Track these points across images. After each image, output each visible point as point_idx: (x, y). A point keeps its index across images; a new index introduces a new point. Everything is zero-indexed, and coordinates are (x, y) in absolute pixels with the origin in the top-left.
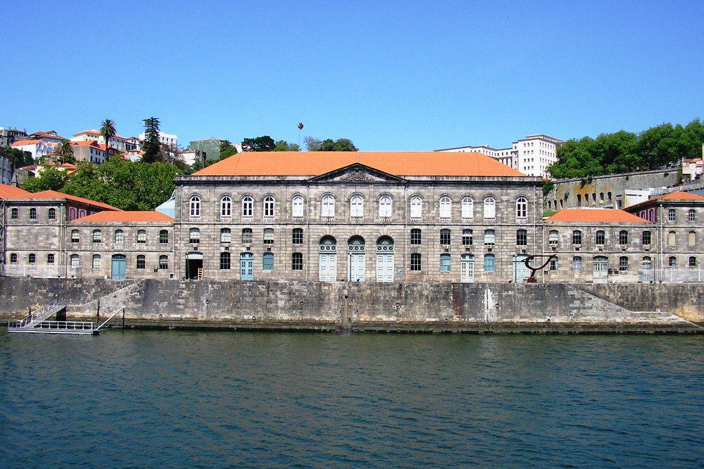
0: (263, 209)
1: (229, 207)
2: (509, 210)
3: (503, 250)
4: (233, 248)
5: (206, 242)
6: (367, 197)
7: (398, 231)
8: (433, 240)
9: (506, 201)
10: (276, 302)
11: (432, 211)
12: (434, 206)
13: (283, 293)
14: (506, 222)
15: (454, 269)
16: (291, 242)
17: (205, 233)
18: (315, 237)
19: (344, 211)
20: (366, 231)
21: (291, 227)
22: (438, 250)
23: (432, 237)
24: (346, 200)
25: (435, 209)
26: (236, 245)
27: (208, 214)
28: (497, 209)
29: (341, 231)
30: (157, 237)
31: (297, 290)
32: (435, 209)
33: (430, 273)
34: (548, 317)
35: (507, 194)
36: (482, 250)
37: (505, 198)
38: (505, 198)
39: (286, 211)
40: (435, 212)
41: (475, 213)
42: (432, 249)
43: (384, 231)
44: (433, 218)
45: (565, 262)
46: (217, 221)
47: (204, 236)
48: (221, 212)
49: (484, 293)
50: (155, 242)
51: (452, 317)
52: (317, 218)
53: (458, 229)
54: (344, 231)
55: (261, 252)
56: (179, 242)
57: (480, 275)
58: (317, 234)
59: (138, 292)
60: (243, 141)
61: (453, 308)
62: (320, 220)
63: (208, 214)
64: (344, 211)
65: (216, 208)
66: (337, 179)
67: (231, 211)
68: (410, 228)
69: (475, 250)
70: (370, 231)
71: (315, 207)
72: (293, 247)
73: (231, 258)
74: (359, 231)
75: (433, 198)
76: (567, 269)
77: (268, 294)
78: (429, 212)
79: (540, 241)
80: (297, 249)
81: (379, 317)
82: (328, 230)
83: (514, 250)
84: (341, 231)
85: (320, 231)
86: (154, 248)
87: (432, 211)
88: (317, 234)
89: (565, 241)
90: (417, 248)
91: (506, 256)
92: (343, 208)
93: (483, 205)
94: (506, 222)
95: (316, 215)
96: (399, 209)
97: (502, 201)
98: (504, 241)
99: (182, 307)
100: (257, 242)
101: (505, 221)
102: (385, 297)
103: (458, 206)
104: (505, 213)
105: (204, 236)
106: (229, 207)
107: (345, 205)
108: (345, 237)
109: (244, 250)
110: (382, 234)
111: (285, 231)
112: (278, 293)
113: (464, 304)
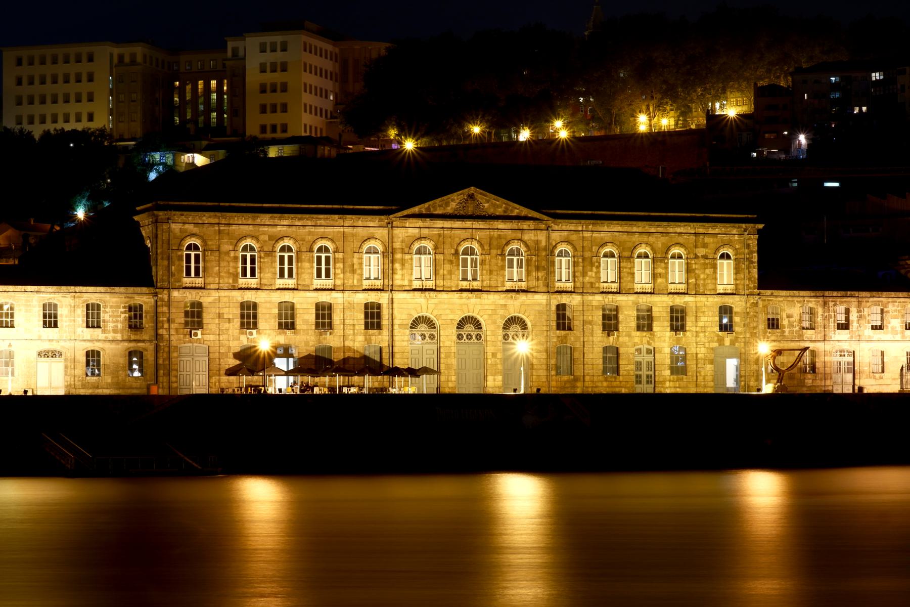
0: (312, 267)
1: (253, 261)
3: (698, 339)
7: (537, 308)
8: (591, 322)
11: (590, 273)
12: (592, 264)
17: (213, 310)
18: (404, 316)
20: (486, 307)
21: (363, 298)
24: (453, 251)
25: (594, 269)
28: (689, 270)
29: (446, 306)
30: (123, 316)
32: (594, 269)
33: (587, 378)
35: (705, 246)
36: (667, 339)
37: (701, 252)
39: (353, 271)
40: (594, 274)
41: (655, 276)
48: (240, 270)
56: (166, 326)
63: (219, 275)
65: (231, 264)
67: (257, 271)
69: (656, 339)
70: (493, 307)
71: (403, 265)
72: (365, 335)
75: (591, 251)
78: (584, 274)
79: (755, 324)
83: (716, 339)
84: (446, 306)
87: (590, 273)
89: (791, 325)
92: (447, 267)
95: (403, 279)
96: (538, 269)
97: (696, 257)
104: (702, 276)
106: (253, 261)
107: (451, 262)
111: (352, 306)
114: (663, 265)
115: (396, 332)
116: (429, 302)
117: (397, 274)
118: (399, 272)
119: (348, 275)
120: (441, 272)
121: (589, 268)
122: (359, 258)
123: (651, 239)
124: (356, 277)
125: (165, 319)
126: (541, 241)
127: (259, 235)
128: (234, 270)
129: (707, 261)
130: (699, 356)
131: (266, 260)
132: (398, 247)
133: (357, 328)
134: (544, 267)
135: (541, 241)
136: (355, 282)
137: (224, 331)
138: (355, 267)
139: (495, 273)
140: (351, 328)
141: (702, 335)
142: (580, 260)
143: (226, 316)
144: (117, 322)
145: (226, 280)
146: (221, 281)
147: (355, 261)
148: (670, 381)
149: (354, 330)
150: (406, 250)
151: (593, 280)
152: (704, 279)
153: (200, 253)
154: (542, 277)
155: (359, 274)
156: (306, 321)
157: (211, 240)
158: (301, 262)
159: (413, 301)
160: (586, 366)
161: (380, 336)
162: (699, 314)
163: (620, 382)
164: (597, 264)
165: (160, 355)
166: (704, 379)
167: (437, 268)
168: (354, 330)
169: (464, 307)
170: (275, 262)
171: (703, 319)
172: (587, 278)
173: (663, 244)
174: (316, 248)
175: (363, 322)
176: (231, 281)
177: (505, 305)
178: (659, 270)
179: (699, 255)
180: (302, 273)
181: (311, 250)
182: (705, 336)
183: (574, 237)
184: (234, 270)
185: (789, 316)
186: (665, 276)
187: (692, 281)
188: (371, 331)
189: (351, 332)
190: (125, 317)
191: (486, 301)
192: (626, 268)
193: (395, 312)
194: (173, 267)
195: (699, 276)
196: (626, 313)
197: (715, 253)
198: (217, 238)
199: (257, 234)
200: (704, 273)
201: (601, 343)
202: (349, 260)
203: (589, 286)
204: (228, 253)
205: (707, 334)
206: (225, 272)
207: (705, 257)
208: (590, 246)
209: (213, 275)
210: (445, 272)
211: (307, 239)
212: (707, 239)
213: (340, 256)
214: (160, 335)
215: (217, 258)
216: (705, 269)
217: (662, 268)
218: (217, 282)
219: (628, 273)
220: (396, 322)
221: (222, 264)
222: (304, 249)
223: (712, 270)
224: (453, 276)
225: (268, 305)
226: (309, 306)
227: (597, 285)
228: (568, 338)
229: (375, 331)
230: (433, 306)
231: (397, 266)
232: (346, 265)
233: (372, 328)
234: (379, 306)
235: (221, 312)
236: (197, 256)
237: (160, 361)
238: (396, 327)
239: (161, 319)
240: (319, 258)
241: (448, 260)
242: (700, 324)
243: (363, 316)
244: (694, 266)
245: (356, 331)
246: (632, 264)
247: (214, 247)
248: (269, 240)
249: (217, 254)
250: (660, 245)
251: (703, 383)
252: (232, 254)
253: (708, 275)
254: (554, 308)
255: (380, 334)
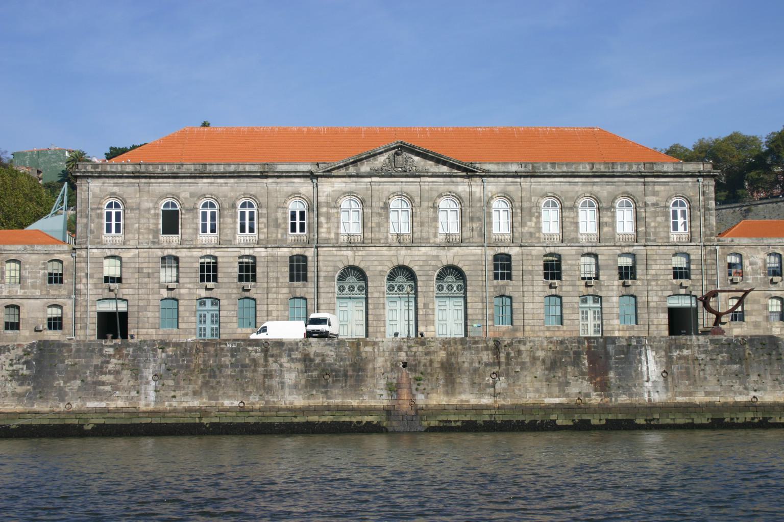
0: (235, 222)
2: (659, 219)
3: (650, 288)
4: (183, 291)
5: (133, 281)
6: (417, 200)
7: (472, 258)
8: (531, 273)
9: (653, 205)
10: (281, 376)
11: (529, 224)
13: (292, 360)
14: (655, 241)
15: (569, 322)
16: (288, 279)
17: (133, 265)
18: (330, 269)
19: (379, 225)
21: (285, 252)
22: (540, 289)
23: (530, 268)
24: (381, 204)
25: (534, 219)
26: (188, 286)
27: (138, 231)
29: (374, 258)
31: (317, 354)
32: (534, 219)
33: (527, 328)
34: (754, 394)
35: (655, 194)
36: (615, 288)
38: (651, 200)
40: (533, 225)
41: (600, 225)
42: (531, 288)
43: (449, 257)
44: (531, 234)
45: (756, 307)
46: (154, 243)
47: (130, 271)
49: (640, 354)
50: (39, 281)
51: (588, 395)
52: (332, 236)
53: (574, 252)
54: (379, 258)
55: (234, 296)
56: (84, 281)
57: (613, 331)
58: (331, 264)
59: (24, 363)
60: (108, 151)
61: (590, 380)
62: (337, 239)
63: (138, 231)
64: (379, 225)
65: (152, 221)
66: (365, 168)
68: (491, 252)
69: (603, 288)
70: (424, 258)
72: (289, 287)
73: (181, 308)
74: (405, 257)
76: (760, 319)
77: (266, 360)
78: (523, 224)
79: (713, 272)
80: (298, 290)
81: (464, 397)
82: (350, 257)
83: (669, 287)
84: (374, 258)
85: (337, 259)
86: (38, 293)
87: (529, 224)
88: (331, 264)
89: (755, 272)
90: (504, 286)
91: (655, 299)
92: (376, 219)
93: (614, 212)
94: (655, 241)
95: (329, 233)
98: (653, 272)
99: (108, 388)
100: (226, 280)
101: (652, 238)
102: (471, 363)
103: (572, 215)
104: (653, 224)
105: (130, 271)
107: (380, 215)
108: (380, 268)
109: (203, 293)
110: (445, 263)
111: (275, 260)
112: (284, 360)
113: (606, 373)
114: (609, 214)
115: (321, 284)
116: (357, 254)
117: (322, 227)
118: (325, 226)
119: (272, 229)
120: (369, 225)
121: (528, 218)
122: (283, 213)
123: (596, 189)
124: (280, 231)
125: (83, 274)
126: (475, 192)
127: (179, 193)
128: (154, 226)
129: (658, 210)
130: (651, 304)
131: (187, 216)
132: (323, 201)
133: (281, 280)
134: (478, 218)
135: (475, 192)
136: (279, 236)
137: (143, 285)
138: (280, 221)
139: (426, 225)
140: (275, 280)
141: (653, 283)
142: (519, 211)
143: (145, 271)
144: (36, 278)
145: (146, 236)
146: (141, 237)
147: (279, 215)
148: (619, 330)
149: (277, 282)
150: (333, 204)
151: (532, 230)
152: (655, 227)
153: (121, 211)
154: (477, 228)
155: (283, 229)
156: (228, 275)
157: (131, 198)
158: (223, 218)
159: (339, 253)
160: (526, 316)
161: (305, 289)
162: (650, 262)
163: (564, 331)
164: (536, 214)
165: (78, 309)
166: (657, 328)
167: (365, 220)
168: (277, 282)
169: (394, 259)
170: (197, 218)
171: (654, 267)
172: (526, 228)
173: (609, 193)
174: (239, 203)
175: (288, 274)
176: (151, 237)
177: (438, 256)
178: (605, 219)
179: (649, 203)
180: (224, 228)
181: (234, 206)
182: (657, 285)
183: (511, 188)
184: (154, 226)
185: (751, 264)
186: (613, 225)
187: (642, 229)
188: (295, 283)
189: (275, 285)
190: (44, 273)
191: (416, 253)
192: (569, 217)
193: (321, 264)
194: (92, 225)
195: (649, 224)
196: (570, 262)
197: (667, 201)
198: (137, 196)
199: (178, 191)
200: (654, 221)
201: (543, 293)
202: (273, 215)
203: (528, 236)
204: (149, 209)
205: (659, 282)
206: (145, 229)
207: (655, 205)
208: (528, 196)
209: (133, 231)
210: (374, 225)
211: (229, 196)
212: (657, 188)
213: (261, 211)
214: (78, 289)
215: (137, 215)
216: (656, 217)
217: (608, 217)
218: (137, 238)
219: (571, 222)
220: (322, 274)
221: (142, 221)
222: (226, 205)
223: (663, 218)
224: (382, 228)
225: (190, 260)
226: (231, 260)
227: (537, 235)
228: (507, 287)
229: (301, 283)
230: (360, 258)
231: (322, 219)
232: (270, 220)
233: (298, 280)
234: (305, 258)
235: (141, 266)
236: (118, 214)
237: (78, 315)
238: (321, 279)
239: (79, 274)
240: (243, 214)
241: (376, 213)
242: (652, 272)
243: (287, 269)
244: (643, 215)
245: (280, 284)
246: (576, 213)
247: (135, 206)
248: (190, 197)
249: (137, 212)
250: (605, 194)
251: (656, 332)
252: (152, 212)
253: (659, 223)
254: (490, 258)
255: (304, 286)
